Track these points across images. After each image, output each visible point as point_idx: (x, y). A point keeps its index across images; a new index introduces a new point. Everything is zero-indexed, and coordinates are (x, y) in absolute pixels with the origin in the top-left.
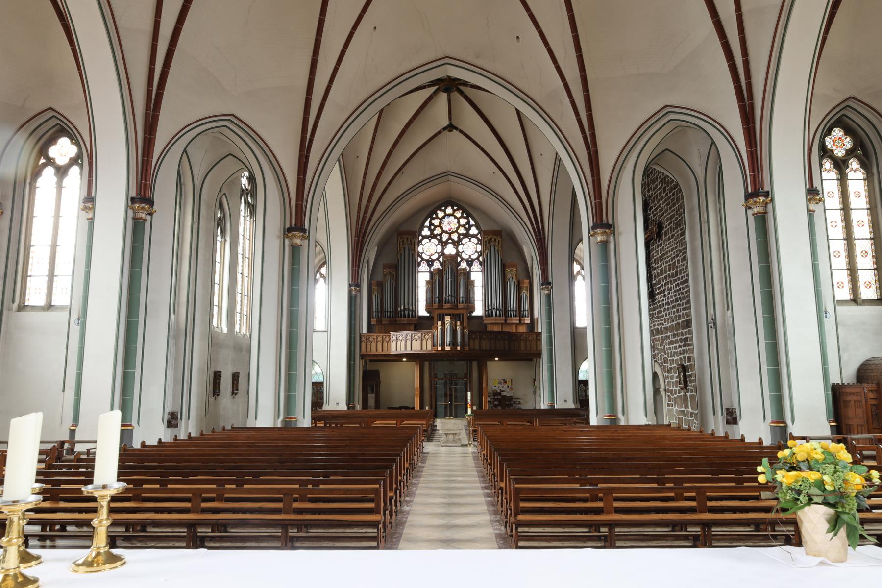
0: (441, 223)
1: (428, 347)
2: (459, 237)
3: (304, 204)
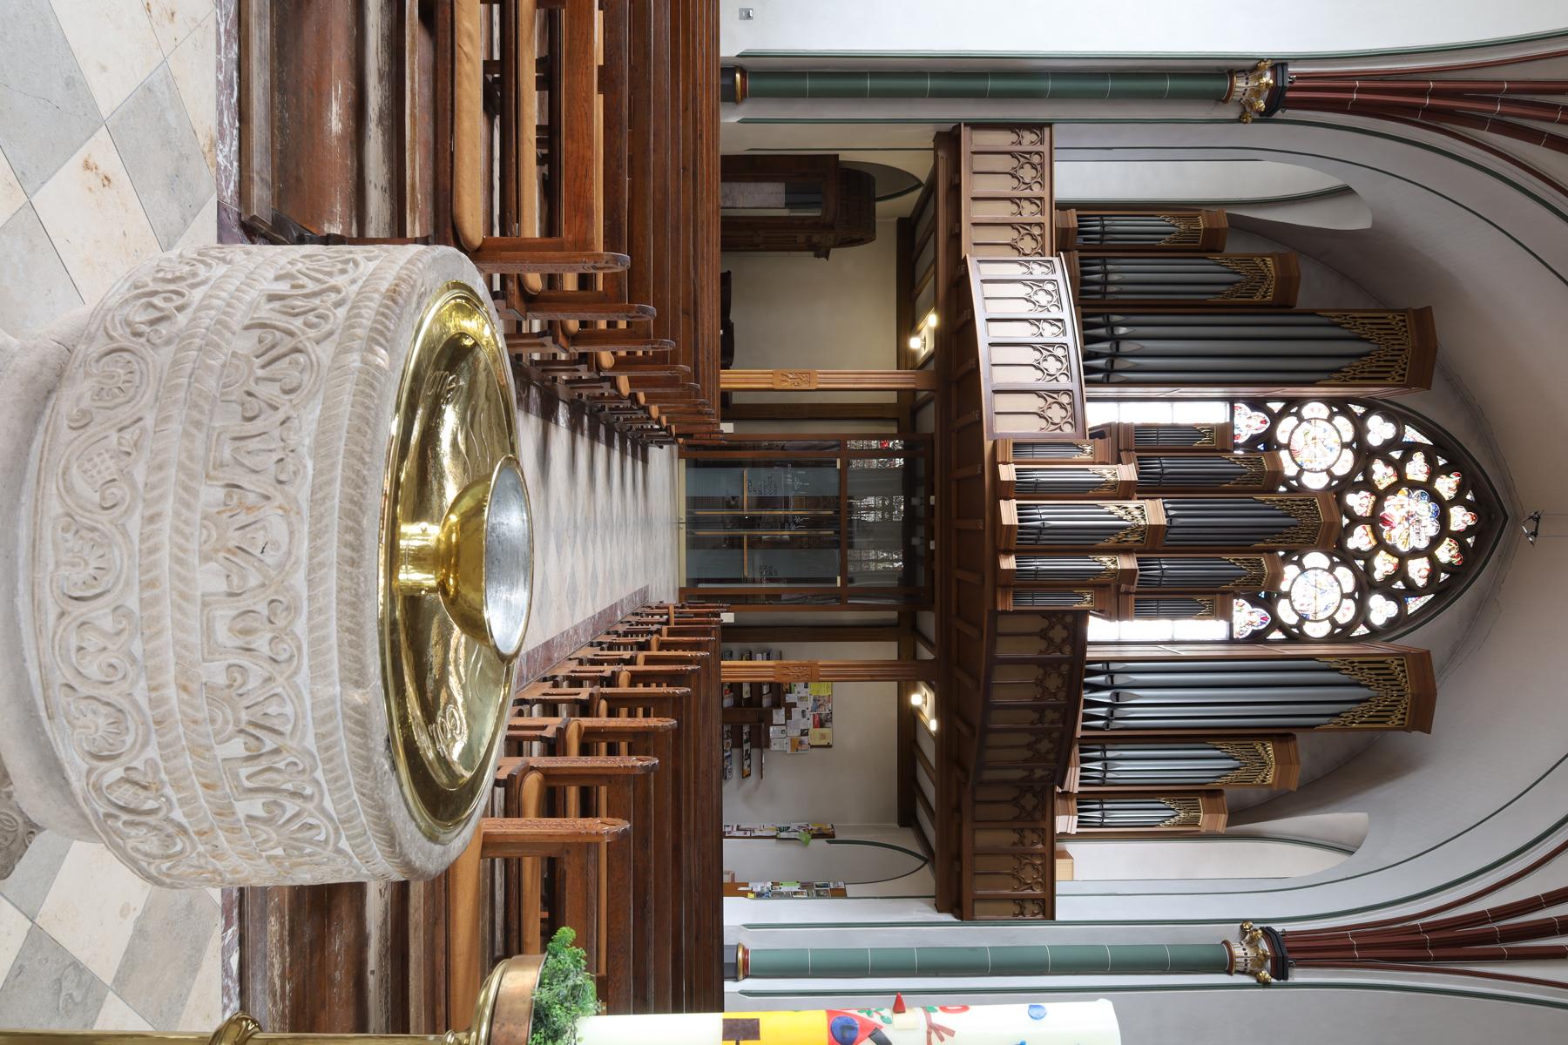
0: (1414, 485)
1: (1008, 418)
2: (1358, 553)
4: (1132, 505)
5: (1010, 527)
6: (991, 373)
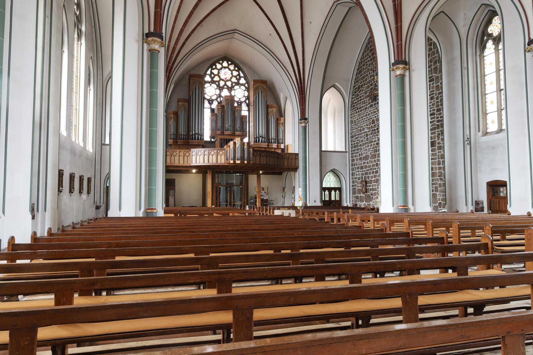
0: (219, 73)
1: (222, 160)
2: (232, 85)
3: (162, 12)
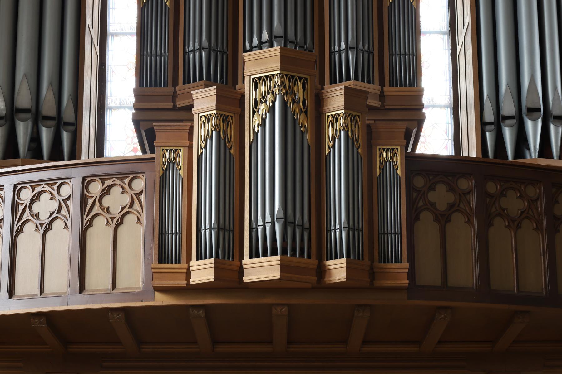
1: (123, 270)
4: (251, 94)
5: (284, 267)
6: (54, 296)
